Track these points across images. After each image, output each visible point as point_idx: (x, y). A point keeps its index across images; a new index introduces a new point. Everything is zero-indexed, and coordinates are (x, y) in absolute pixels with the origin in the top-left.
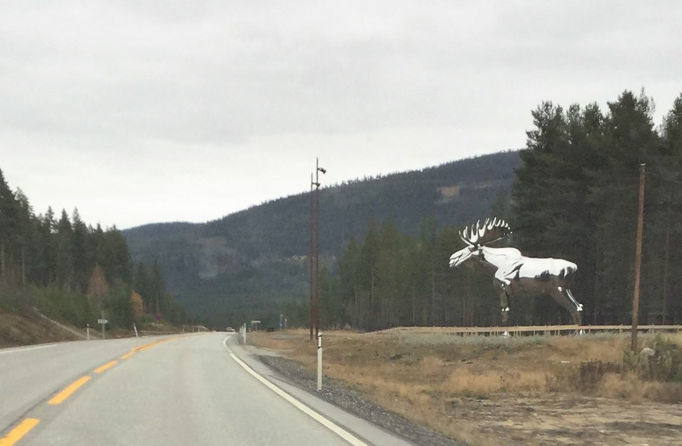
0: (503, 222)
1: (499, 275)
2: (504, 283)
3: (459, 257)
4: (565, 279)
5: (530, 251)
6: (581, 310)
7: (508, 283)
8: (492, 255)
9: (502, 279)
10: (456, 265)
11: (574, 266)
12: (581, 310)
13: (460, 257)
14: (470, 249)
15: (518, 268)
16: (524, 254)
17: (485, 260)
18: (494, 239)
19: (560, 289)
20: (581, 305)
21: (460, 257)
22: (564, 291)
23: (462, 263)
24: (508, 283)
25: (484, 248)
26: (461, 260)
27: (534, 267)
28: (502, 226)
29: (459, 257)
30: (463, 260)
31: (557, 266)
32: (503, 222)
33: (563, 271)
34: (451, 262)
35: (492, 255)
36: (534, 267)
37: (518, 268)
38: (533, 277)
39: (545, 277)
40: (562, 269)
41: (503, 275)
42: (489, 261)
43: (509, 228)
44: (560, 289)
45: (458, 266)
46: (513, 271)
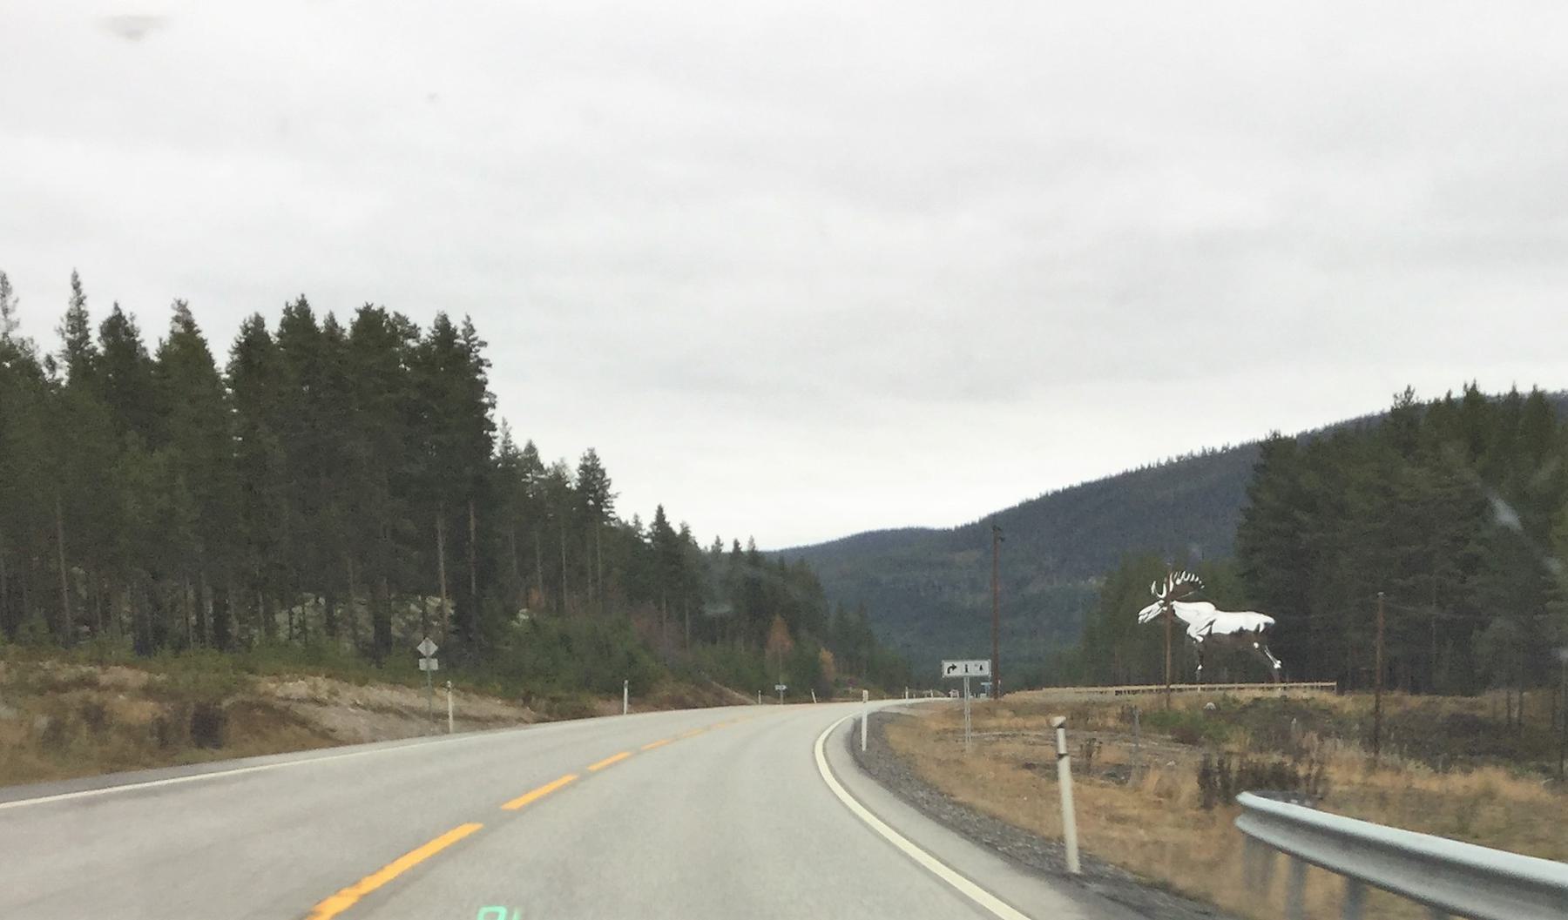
0: (1193, 576)
1: (1192, 631)
2: (1195, 639)
3: (1149, 613)
4: (1268, 634)
5: (1223, 606)
6: (1279, 666)
7: (1200, 639)
8: (1184, 610)
9: (1193, 635)
10: (1146, 621)
11: (1271, 620)
12: (1279, 666)
13: (1149, 613)
14: (1160, 605)
15: (1211, 623)
16: (1218, 608)
17: (1175, 615)
18: (1190, 594)
19: (1256, 645)
20: (1279, 662)
21: (1149, 613)
22: (1261, 649)
23: (1152, 620)
24: (1200, 639)
25: (1175, 603)
26: (1151, 616)
27: (1229, 622)
28: (1192, 579)
29: (1149, 613)
30: (1153, 616)
31: (1253, 621)
32: (1193, 576)
33: (1258, 626)
34: (1140, 618)
35: (1184, 610)
36: (1229, 622)
37: (1211, 623)
38: (1228, 632)
39: (1241, 633)
40: (1257, 623)
41: (1196, 631)
42: (1180, 617)
43: (1200, 582)
44: (1256, 645)
45: (1148, 622)
46: (1207, 626)
